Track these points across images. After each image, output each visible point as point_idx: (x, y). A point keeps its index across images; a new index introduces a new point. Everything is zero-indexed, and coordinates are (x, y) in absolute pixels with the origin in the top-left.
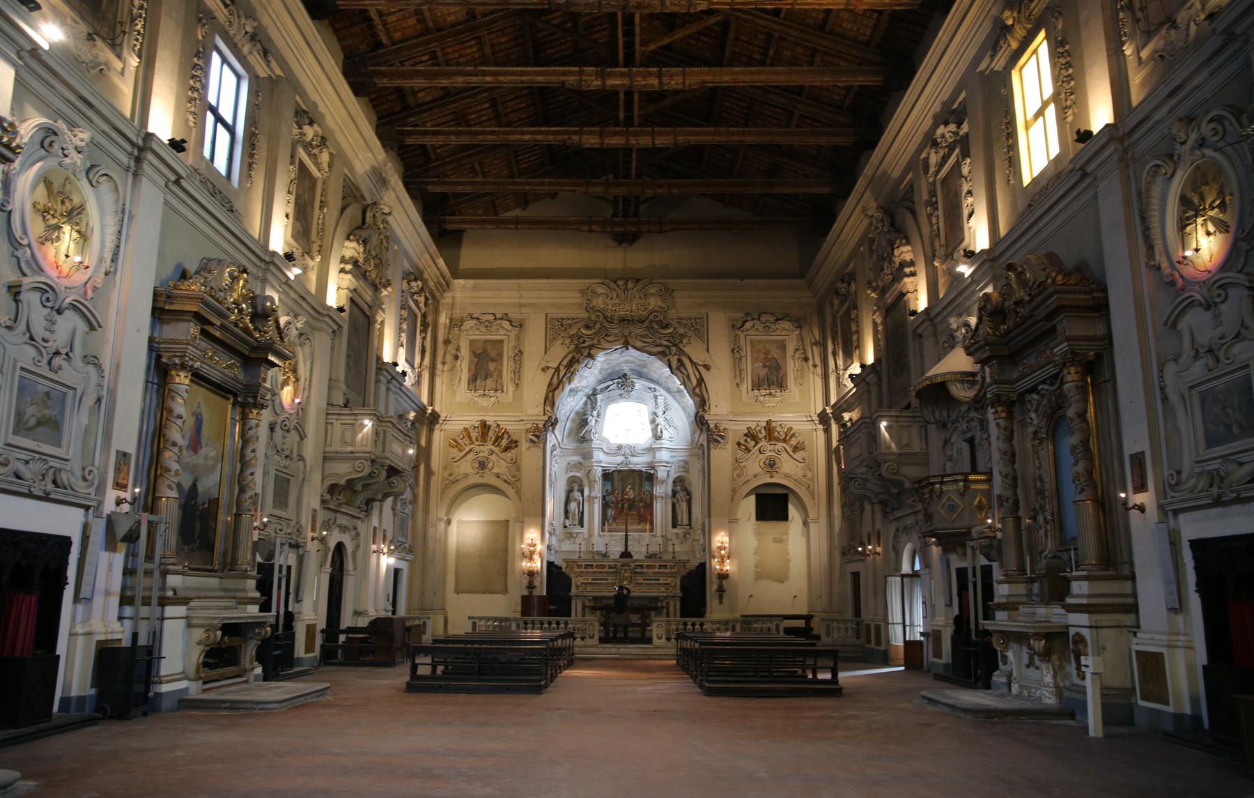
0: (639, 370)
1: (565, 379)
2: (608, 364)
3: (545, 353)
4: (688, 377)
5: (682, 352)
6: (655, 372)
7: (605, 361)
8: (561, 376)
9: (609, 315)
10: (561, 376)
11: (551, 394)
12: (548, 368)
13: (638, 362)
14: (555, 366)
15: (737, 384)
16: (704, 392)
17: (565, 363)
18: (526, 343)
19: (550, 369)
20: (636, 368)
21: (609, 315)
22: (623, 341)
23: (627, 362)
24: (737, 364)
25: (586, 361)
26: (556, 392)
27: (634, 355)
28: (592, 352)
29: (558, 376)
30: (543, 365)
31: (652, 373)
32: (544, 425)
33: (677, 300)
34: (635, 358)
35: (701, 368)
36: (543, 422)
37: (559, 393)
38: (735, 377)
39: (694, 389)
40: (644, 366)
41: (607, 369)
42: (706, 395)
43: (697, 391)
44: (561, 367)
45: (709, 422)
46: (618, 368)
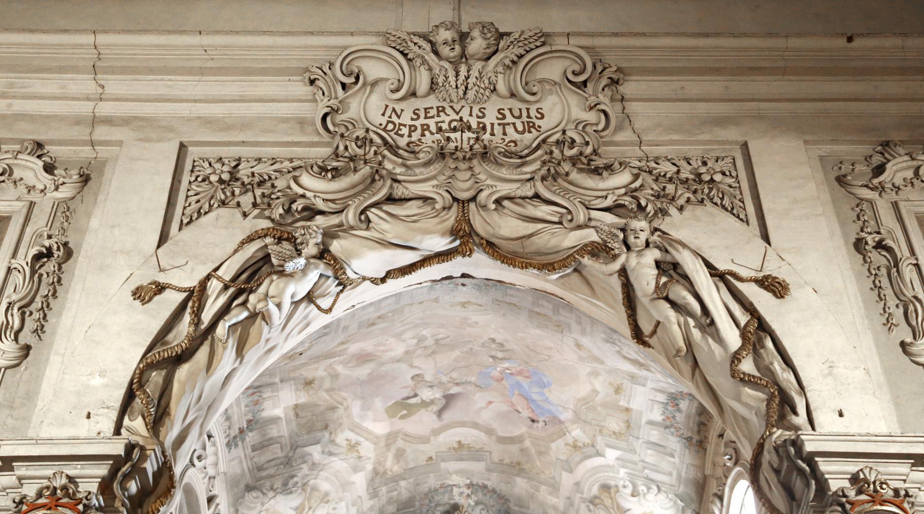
0: (502, 488)
1: (221, 330)
2: (400, 454)
3: (163, 239)
4: (708, 324)
5: (665, 243)
6: (555, 487)
7: (391, 437)
8: (207, 316)
9: (402, 142)
10: (207, 316)
11: (156, 377)
12: (160, 288)
13: (497, 452)
14: (192, 282)
15: (903, 344)
16: (778, 366)
17: (227, 273)
18: (94, 223)
19: (168, 293)
20: (493, 481)
21: (402, 142)
22: (451, 218)
23: (461, 451)
24: (885, 282)
25: (313, 276)
26: (183, 372)
27: (486, 417)
28: (336, 247)
29: (197, 313)
30: (145, 277)
31: (543, 492)
32: (106, 486)
33: (633, 107)
34: (489, 432)
35: (752, 291)
36: (102, 470)
37: (192, 377)
38: (889, 324)
39: (736, 358)
40: (516, 468)
41: (396, 479)
42: (785, 377)
43: (747, 366)
44: (214, 286)
45: (824, 466)
46: (432, 482)
